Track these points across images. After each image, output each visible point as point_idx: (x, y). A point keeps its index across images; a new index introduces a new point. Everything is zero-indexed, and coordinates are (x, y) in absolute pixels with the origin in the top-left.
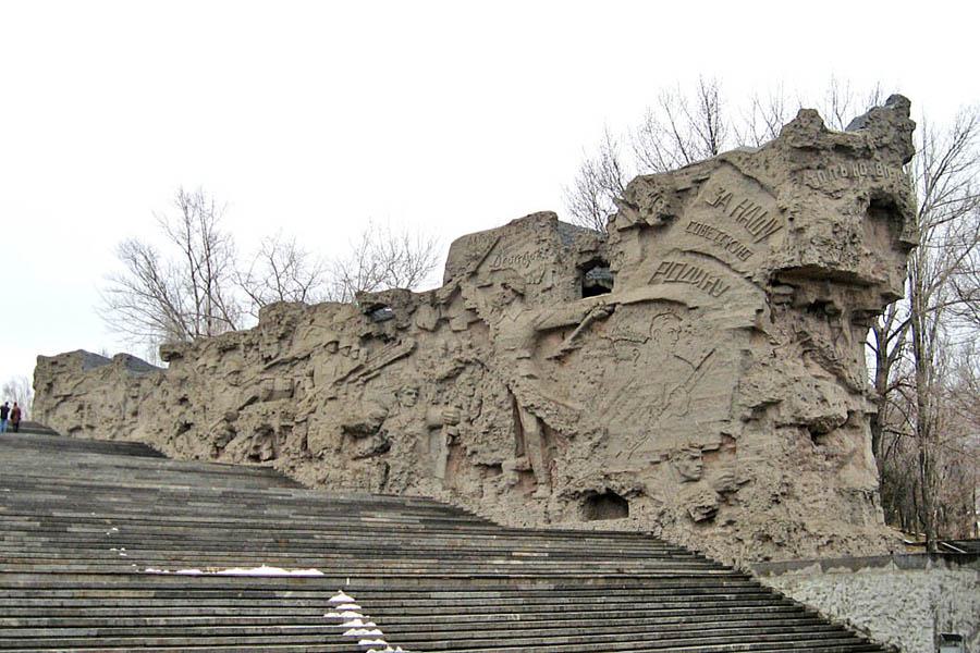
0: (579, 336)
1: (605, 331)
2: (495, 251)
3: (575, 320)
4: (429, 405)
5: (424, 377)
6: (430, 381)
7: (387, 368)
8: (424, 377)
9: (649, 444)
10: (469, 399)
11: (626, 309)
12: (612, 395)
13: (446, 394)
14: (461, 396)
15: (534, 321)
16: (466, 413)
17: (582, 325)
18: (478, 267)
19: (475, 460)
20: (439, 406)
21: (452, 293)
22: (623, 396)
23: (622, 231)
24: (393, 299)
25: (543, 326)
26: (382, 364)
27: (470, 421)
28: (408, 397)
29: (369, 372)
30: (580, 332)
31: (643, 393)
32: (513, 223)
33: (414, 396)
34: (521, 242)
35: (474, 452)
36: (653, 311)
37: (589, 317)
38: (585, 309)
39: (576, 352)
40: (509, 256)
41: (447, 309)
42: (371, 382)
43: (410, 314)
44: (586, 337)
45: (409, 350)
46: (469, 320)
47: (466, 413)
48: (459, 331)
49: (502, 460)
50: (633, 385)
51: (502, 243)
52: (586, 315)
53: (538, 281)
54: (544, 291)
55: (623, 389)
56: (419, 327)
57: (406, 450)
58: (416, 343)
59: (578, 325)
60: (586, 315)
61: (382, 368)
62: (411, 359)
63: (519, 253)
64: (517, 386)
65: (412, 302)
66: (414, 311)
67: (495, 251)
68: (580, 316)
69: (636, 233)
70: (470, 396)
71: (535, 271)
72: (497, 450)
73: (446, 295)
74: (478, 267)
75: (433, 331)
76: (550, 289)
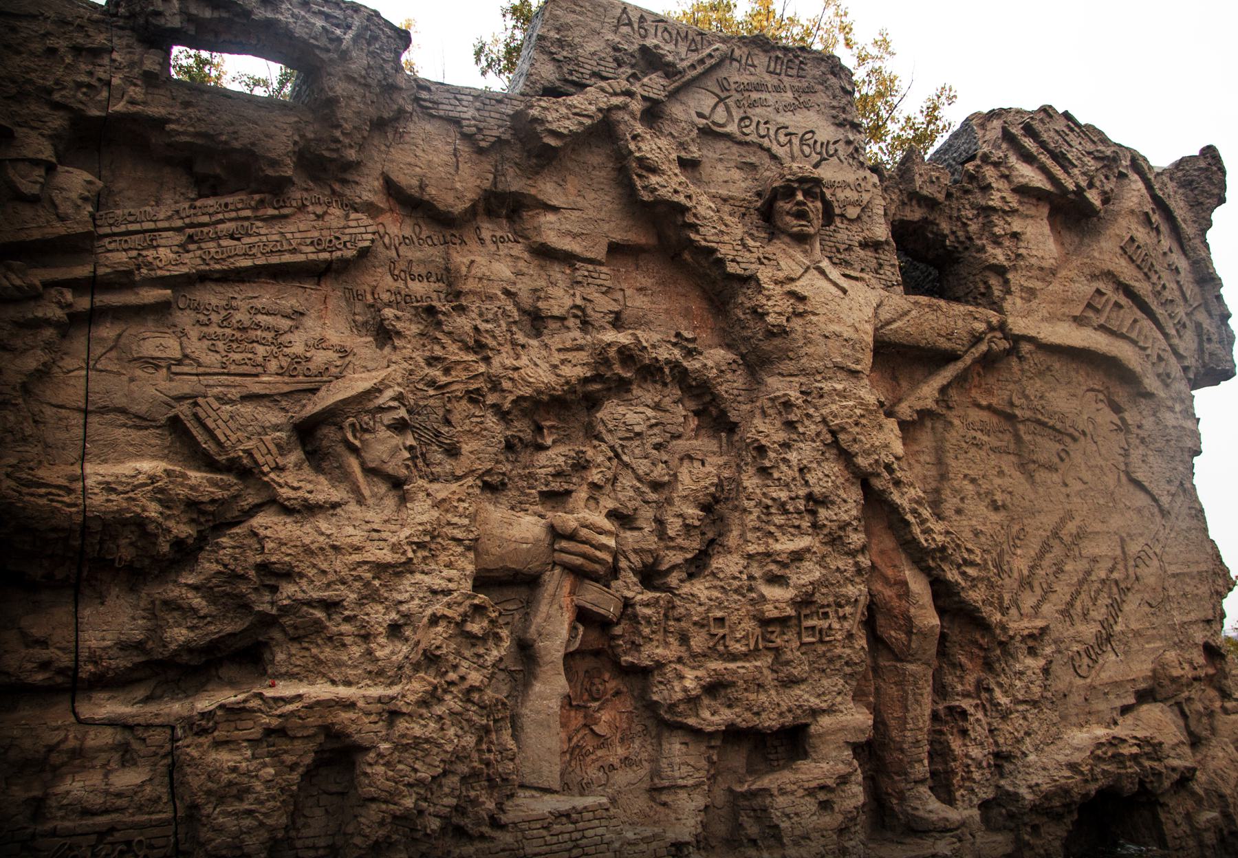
1: (989, 392)
2: (711, 83)
5: (436, 373)
6: (474, 397)
7: (212, 297)
8: (436, 373)
9: (1112, 667)
10: (653, 496)
11: (1040, 357)
12: (1034, 547)
16: (652, 542)
19: (714, 717)
22: (1057, 550)
23: (1023, 191)
24: (355, 40)
26: (190, 263)
27: (650, 576)
28: (397, 440)
29: (125, 280)
31: (1090, 548)
34: (788, 96)
35: (714, 688)
36: (1083, 379)
42: (107, 331)
45: (350, 253)
46: (618, 237)
47: (652, 542)
48: (568, 259)
49: (815, 713)
50: (1071, 527)
55: (1055, 534)
56: (391, 188)
57: (475, 678)
59: (951, 357)
61: (202, 278)
69: (1045, 211)
70: (656, 486)
72: (803, 681)
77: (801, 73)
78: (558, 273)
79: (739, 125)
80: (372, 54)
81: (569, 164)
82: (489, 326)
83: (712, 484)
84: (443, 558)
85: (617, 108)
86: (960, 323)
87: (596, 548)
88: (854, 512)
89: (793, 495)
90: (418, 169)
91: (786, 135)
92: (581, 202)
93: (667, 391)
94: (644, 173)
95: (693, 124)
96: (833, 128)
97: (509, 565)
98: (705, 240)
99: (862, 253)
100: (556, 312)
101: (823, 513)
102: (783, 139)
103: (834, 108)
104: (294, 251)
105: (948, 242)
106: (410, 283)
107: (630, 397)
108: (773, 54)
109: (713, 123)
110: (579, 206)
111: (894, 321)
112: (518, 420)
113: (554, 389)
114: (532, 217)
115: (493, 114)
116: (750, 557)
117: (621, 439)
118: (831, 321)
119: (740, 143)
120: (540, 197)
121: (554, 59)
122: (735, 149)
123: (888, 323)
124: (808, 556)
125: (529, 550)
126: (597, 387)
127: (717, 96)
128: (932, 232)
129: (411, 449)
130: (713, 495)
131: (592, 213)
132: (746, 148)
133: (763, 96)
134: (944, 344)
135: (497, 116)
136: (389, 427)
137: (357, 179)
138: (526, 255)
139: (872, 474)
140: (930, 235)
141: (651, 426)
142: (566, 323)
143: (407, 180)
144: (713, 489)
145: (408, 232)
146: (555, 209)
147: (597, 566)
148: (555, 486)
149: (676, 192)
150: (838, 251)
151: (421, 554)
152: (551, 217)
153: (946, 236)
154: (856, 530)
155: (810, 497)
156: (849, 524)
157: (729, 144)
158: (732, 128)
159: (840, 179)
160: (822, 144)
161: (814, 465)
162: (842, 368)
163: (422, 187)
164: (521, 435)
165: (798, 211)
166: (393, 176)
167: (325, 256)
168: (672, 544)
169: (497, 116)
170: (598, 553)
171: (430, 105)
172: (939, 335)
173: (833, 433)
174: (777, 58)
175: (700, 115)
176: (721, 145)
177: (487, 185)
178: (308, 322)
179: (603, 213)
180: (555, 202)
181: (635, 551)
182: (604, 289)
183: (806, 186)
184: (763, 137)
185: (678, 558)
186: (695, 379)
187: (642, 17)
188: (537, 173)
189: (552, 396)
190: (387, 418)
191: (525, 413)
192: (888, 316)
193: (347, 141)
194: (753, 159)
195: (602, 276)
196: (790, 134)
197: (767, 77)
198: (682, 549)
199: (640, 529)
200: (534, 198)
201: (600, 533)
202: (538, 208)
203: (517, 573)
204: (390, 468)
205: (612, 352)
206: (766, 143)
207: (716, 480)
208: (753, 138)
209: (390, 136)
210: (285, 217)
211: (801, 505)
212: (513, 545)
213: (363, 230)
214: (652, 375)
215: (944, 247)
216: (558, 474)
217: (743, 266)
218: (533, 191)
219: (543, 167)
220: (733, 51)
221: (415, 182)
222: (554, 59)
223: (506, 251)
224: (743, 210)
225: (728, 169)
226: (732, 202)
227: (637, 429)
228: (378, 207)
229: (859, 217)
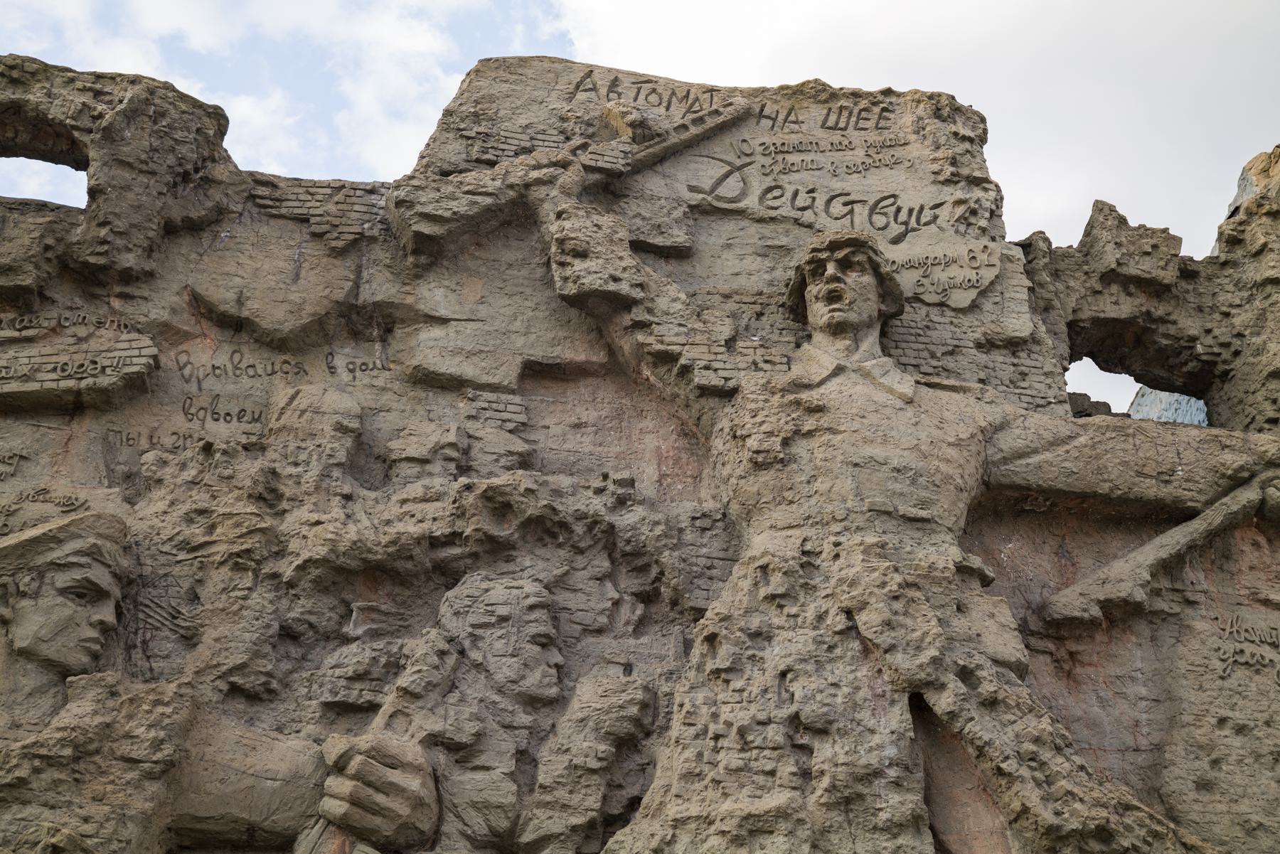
0: (1169, 567)
3: (1190, 496)
4: (207, 692)
5: (196, 533)
6: (238, 562)
10: (524, 718)
13: (353, 656)
14: (475, 688)
15: (990, 433)
16: (506, 793)
17: (1213, 517)
18: (639, 168)
20: (268, 716)
21: (488, 209)
25: (1021, 471)
28: (69, 608)
30: (1191, 547)
32: (817, 92)
33: (106, 613)
37: (1248, 495)
38: (1233, 460)
39: (1143, 627)
40: (790, 183)
41: (419, 273)
43: (170, 230)
44: (1195, 576)
46: (539, 353)
48: (453, 385)
51: (758, 136)
52: (1237, 481)
53: (962, 298)
54: (987, 345)
56: (202, 307)
58: (156, 364)
59: (1177, 514)
60: (1237, 481)
62: (86, 431)
63: (838, 185)
64: (991, 704)
65: (208, 181)
66: (193, 227)
67: (723, 148)
68: (1204, 479)
70: (533, 702)
71: (949, 262)
73: (461, 206)
74: (639, 168)
75: (277, 343)
76: (1014, 345)
77: (882, 123)
78: (441, 403)
79: (762, 198)
80: (161, 135)
81: (470, 264)
82: (292, 470)
83: (631, 702)
84: (97, 786)
85: (539, 182)
86: (1189, 455)
87: (377, 789)
88: (891, 752)
89: (762, 716)
90: (238, 280)
91: (845, 204)
92: (483, 311)
93: (580, 561)
94: (569, 259)
95: (679, 201)
96: (934, 188)
97: (236, 812)
98: (662, 342)
99: (982, 358)
100: (413, 451)
101: (826, 752)
102: (837, 208)
103: (935, 160)
104: (26, 378)
105: (1199, 349)
106: (210, 424)
107: (511, 567)
108: (835, 105)
109: (719, 198)
110: (480, 316)
111: (1035, 451)
112: (309, 597)
113: (369, 551)
114: (409, 334)
115: (356, 208)
116: (678, 823)
117: (473, 626)
118: (866, 441)
119: (761, 220)
120: (421, 306)
121: (462, 136)
122: (753, 229)
123: (1021, 455)
124: (783, 826)
125: (274, 791)
126: (456, 551)
127: (729, 164)
128: (1167, 336)
129: (103, 627)
130: (636, 721)
131: (499, 324)
132: (772, 226)
133: (808, 157)
134: (1150, 489)
135: (364, 209)
136: (63, 592)
137: (146, 294)
138: (397, 386)
139: (929, 684)
140: (1165, 342)
141: (532, 608)
142: (428, 467)
143: (222, 295)
144: (634, 710)
145: (222, 359)
146: (444, 321)
147: (378, 821)
148: (354, 695)
149: (616, 279)
150: (933, 356)
151: (51, 775)
152: (437, 332)
153: (1193, 339)
154: (897, 784)
155: (795, 720)
156: (877, 773)
157: (745, 223)
158: (751, 202)
159: (940, 254)
160: (911, 211)
161: (810, 667)
162: (888, 513)
163: (240, 302)
164: (313, 619)
165: (830, 292)
166: (200, 290)
167: (71, 383)
168: (548, 798)
169: (364, 209)
170: (380, 798)
171: (270, 203)
172: (1139, 474)
173: (849, 613)
174: (841, 108)
175: (692, 189)
176: (728, 227)
177: (339, 295)
178: (29, 468)
179: (518, 323)
180: (443, 312)
181: (474, 805)
182: (511, 426)
183: (840, 254)
184: (803, 209)
185: (557, 823)
186: (628, 542)
187: (616, 79)
188: (418, 277)
189: (365, 560)
190: (63, 579)
191: (321, 587)
192: (1020, 444)
193: (119, 242)
194: (783, 241)
195: (510, 408)
196: (853, 202)
197: (821, 134)
198: (565, 807)
199: (487, 769)
200: (410, 308)
201: (393, 767)
202: (416, 321)
203: (252, 829)
204: (49, 651)
205: (470, 499)
206: (808, 216)
207: (639, 695)
208: (786, 211)
209: (206, 243)
210: (29, 340)
211: (775, 734)
212: (249, 781)
213: (136, 352)
214: (554, 536)
215: (1197, 357)
216: (358, 677)
217: (721, 373)
218: (409, 300)
219: (429, 267)
220: (763, 107)
221: (231, 296)
222: (462, 136)
223: (366, 381)
224: (758, 308)
225: (741, 257)
226: (737, 298)
227: (502, 611)
228: (178, 331)
229: (974, 307)
